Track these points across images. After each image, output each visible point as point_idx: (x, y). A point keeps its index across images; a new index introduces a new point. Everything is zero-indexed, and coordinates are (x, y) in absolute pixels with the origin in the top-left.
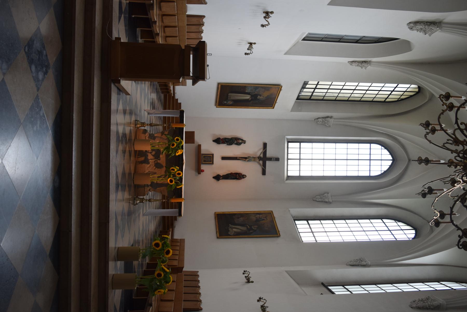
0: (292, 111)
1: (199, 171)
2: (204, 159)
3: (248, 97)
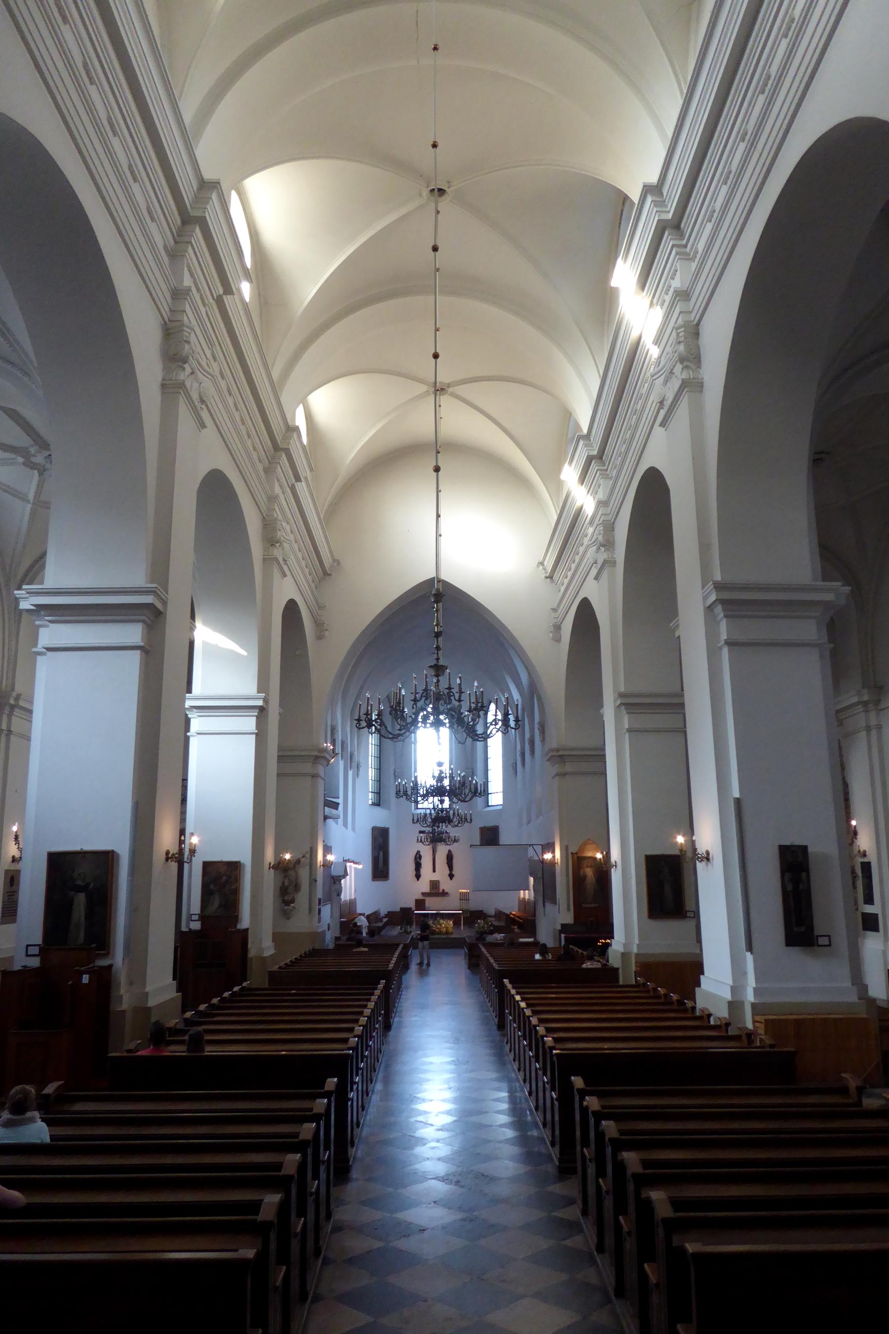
0: (389, 809)
1: (444, 894)
2: (435, 890)
3: (381, 853)
